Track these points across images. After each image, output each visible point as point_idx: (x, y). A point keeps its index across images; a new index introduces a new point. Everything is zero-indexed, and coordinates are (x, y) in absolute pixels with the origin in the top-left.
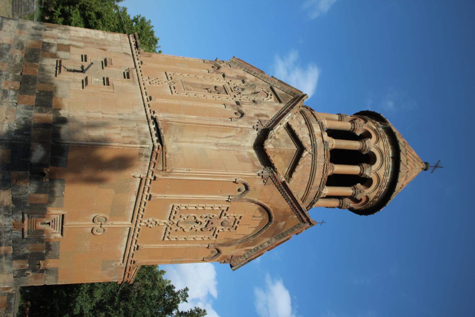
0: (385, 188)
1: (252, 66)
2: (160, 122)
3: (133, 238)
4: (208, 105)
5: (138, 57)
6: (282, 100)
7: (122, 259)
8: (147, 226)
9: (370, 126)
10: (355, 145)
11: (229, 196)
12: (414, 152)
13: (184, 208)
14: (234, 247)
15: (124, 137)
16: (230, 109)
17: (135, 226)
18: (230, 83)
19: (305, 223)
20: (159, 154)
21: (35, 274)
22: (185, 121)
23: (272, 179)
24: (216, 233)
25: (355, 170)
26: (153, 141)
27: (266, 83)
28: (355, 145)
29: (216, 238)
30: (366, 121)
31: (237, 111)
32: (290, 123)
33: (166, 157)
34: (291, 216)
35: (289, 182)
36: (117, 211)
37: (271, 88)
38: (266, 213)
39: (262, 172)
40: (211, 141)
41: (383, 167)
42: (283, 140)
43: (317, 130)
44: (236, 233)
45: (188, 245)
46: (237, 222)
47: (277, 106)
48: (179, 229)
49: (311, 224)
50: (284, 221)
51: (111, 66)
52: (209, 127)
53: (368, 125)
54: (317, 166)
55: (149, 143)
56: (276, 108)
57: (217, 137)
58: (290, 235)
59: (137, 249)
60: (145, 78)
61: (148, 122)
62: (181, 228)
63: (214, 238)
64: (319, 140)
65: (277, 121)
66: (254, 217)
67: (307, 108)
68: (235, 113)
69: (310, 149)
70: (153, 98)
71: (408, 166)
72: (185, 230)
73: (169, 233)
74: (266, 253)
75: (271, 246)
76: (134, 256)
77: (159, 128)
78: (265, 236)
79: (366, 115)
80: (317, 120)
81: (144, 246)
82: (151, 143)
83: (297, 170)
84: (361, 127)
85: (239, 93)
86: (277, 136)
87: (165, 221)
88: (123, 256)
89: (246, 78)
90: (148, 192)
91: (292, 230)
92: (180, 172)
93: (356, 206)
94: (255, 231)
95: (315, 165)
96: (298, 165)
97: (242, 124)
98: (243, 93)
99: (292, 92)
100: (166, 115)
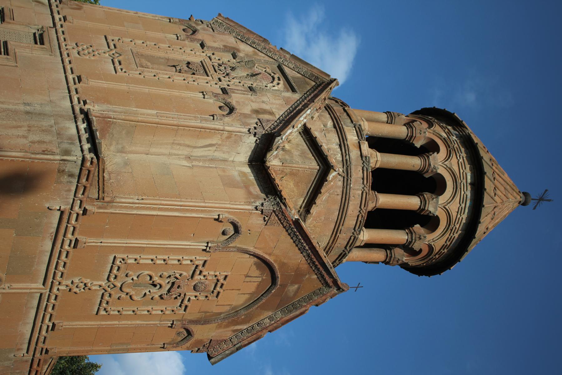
0: (460, 232)
1: (248, 30)
2: (94, 118)
3: (45, 311)
4: (176, 93)
5: (59, 9)
6: (296, 88)
7: (26, 345)
8: (70, 290)
9: (437, 132)
10: (412, 163)
11: (208, 243)
12: (506, 177)
13: (132, 261)
14: (214, 325)
15: (32, 142)
16: (211, 101)
17: (50, 291)
18: (213, 57)
19: (330, 287)
20: (92, 173)
22: (137, 119)
23: (277, 216)
24: (186, 302)
25: (411, 202)
26: (82, 151)
27: (272, 60)
28: (412, 163)
29: (185, 310)
30: (431, 125)
31: (223, 105)
32: (309, 126)
33: (104, 177)
34: (307, 276)
35: (304, 221)
36: (18, 267)
37: (280, 68)
38: (267, 270)
39: (262, 205)
40: (180, 152)
41: (457, 199)
42: (296, 153)
43: (352, 137)
45: (138, 322)
46: (219, 285)
47: (289, 98)
48: (123, 295)
49: (339, 288)
50: (296, 283)
51: (12, 21)
52: (177, 129)
53: (434, 131)
54: (351, 195)
55: (75, 154)
56: (287, 100)
57: (188, 146)
58: (305, 306)
59: (53, 329)
60: (71, 44)
61: (75, 118)
62: (127, 294)
63: (182, 312)
64: (354, 154)
65: (287, 121)
66: (247, 276)
67: (337, 102)
68: (220, 108)
69: (339, 168)
70: (83, 77)
71: (496, 198)
72: (135, 298)
73: (107, 303)
74: (267, 336)
75: (275, 325)
76: (47, 341)
77: (94, 128)
78: (264, 308)
79: (432, 115)
80: (352, 122)
81: (64, 324)
82: (80, 154)
83: (318, 201)
84: (423, 134)
85: (228, 75)
86: (287, 146)
87: (100, 283)
88: (27, 341)
89: (239, 50)
90: (73, 234)
91: (309, 299)
92: (127, 202)
93: (412, 261)
95: (349, 195)
96: (321, 193)
97: (231, 124)
98: (233, 74)
99: (312, 75)
100: (105, 107)
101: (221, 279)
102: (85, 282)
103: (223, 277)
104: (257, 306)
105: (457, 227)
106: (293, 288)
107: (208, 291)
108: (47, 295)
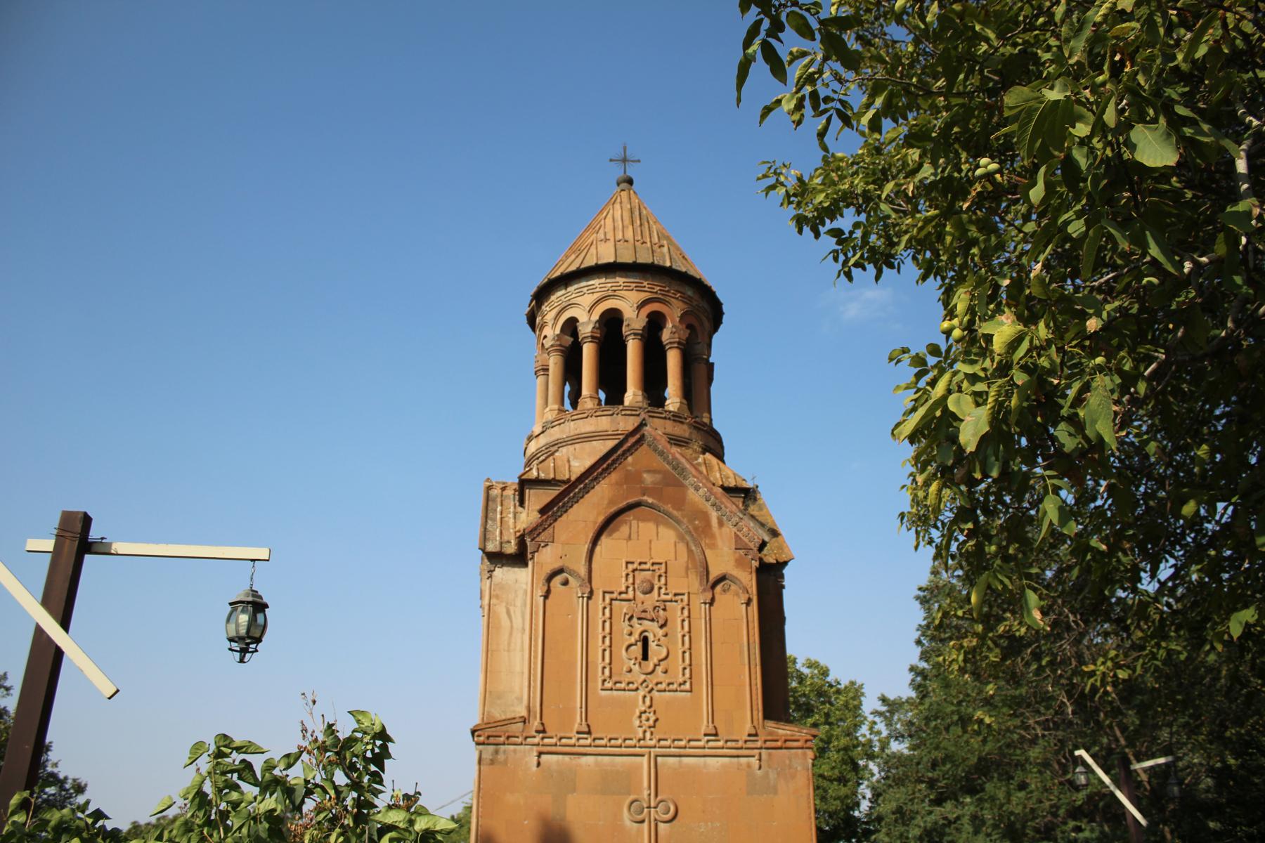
0: (618, 279)
13: (607, 672)
38: (621, 518)
40: (519, 641)
44: (672, 556)
46: (643, 567)
48: (659, 669)
57: (511, 634)
58: (673, 455)
59: (716, 735)
64: (543, 440)
66: (630, 538)
72: (664, 654)
78: (680, 503)
93: (674, 313)
94: (667, 525)
101: (631, 567)
104: (675, 513)
107: (653, 576)
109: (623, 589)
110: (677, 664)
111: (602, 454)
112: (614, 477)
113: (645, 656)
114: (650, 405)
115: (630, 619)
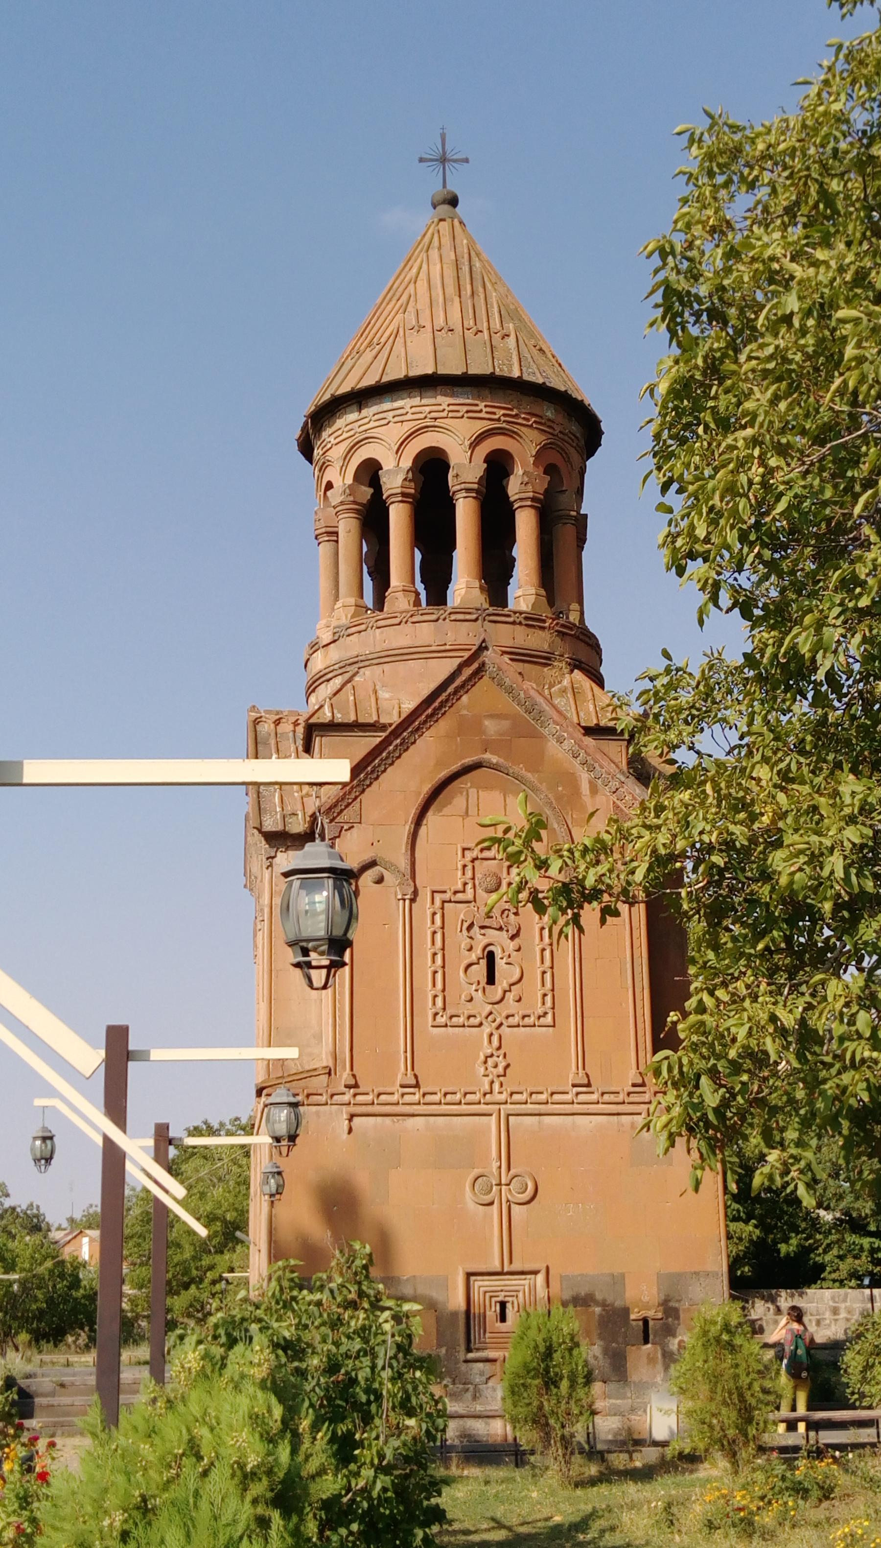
0: (440, 399)
13: (439, 1002)
17: (506, 1103)
21: (681, 1329)
23: (342, 811)
34: (465, 712)
38: (456, 784)
48: (510, 996)
59: (589, 1085)
75: (570, 729)
101: (469, 855)
102: (482, 1058)
103: (466, 852)
104: (529, 775)
105: (428, 409)
106: (491, 727)
108: (513, 1106)
109: (460, 887)
110: (534, 988)
111: (425, 692)
112: (443, 726)
113: (491, 979)
114: (491, 605)
115: (469, 928)
